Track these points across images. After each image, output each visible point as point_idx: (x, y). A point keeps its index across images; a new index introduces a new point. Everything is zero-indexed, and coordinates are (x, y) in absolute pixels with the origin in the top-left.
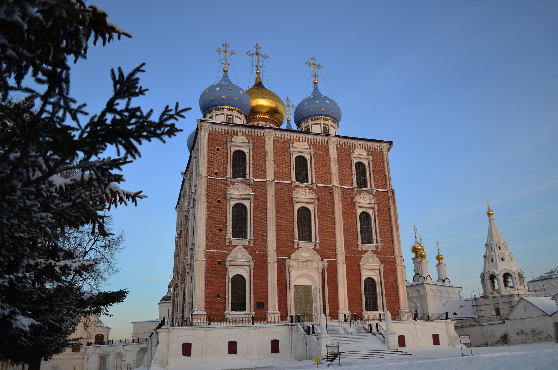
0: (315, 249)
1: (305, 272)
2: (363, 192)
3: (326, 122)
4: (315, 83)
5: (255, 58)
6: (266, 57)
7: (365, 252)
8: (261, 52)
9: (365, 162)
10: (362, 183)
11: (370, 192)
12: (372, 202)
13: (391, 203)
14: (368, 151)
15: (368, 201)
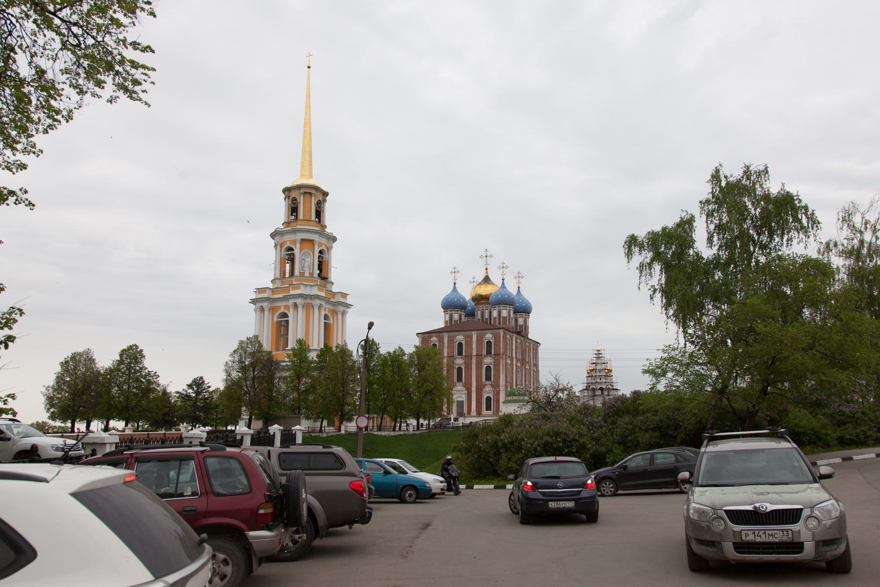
0: (463, 385)
1: (460, 395)
2: (487, 356)
3: (499, 308)
4: (503, 280)
5: (485, 258)
6: (491, 256)
7: (486, 385)
8: (489, 254)
9: (491, 341)
10: (489, 353)
11: (492, 356)
12: (492, 361)
13: (501, 360)
14: (492, 335)
15: (490, 361)
